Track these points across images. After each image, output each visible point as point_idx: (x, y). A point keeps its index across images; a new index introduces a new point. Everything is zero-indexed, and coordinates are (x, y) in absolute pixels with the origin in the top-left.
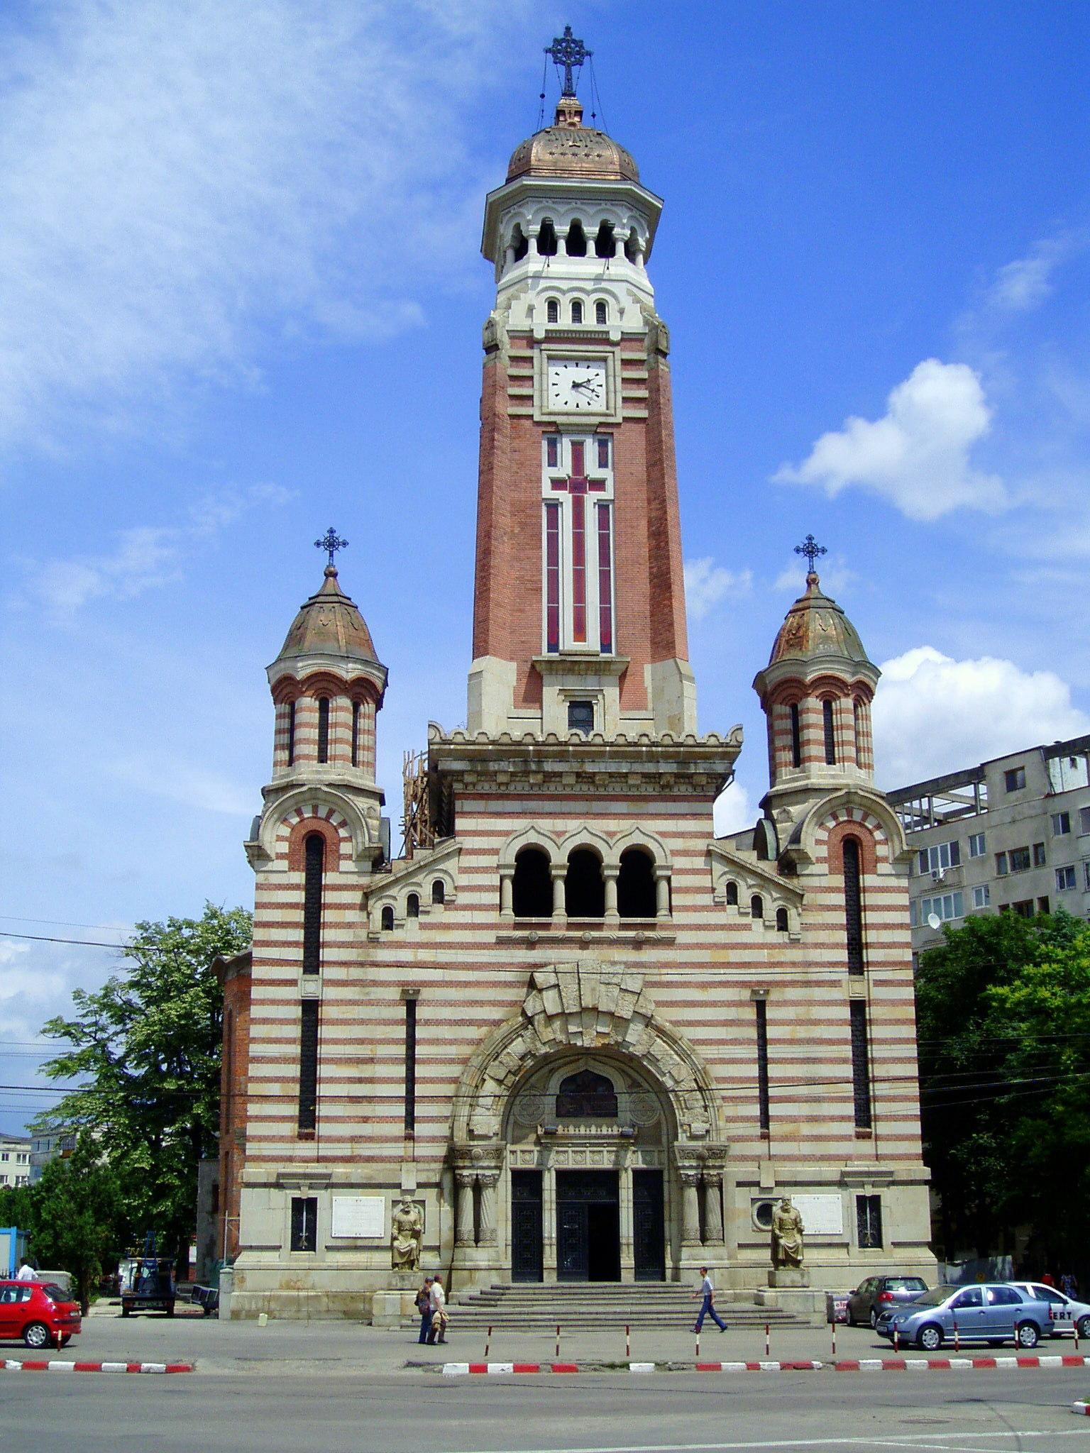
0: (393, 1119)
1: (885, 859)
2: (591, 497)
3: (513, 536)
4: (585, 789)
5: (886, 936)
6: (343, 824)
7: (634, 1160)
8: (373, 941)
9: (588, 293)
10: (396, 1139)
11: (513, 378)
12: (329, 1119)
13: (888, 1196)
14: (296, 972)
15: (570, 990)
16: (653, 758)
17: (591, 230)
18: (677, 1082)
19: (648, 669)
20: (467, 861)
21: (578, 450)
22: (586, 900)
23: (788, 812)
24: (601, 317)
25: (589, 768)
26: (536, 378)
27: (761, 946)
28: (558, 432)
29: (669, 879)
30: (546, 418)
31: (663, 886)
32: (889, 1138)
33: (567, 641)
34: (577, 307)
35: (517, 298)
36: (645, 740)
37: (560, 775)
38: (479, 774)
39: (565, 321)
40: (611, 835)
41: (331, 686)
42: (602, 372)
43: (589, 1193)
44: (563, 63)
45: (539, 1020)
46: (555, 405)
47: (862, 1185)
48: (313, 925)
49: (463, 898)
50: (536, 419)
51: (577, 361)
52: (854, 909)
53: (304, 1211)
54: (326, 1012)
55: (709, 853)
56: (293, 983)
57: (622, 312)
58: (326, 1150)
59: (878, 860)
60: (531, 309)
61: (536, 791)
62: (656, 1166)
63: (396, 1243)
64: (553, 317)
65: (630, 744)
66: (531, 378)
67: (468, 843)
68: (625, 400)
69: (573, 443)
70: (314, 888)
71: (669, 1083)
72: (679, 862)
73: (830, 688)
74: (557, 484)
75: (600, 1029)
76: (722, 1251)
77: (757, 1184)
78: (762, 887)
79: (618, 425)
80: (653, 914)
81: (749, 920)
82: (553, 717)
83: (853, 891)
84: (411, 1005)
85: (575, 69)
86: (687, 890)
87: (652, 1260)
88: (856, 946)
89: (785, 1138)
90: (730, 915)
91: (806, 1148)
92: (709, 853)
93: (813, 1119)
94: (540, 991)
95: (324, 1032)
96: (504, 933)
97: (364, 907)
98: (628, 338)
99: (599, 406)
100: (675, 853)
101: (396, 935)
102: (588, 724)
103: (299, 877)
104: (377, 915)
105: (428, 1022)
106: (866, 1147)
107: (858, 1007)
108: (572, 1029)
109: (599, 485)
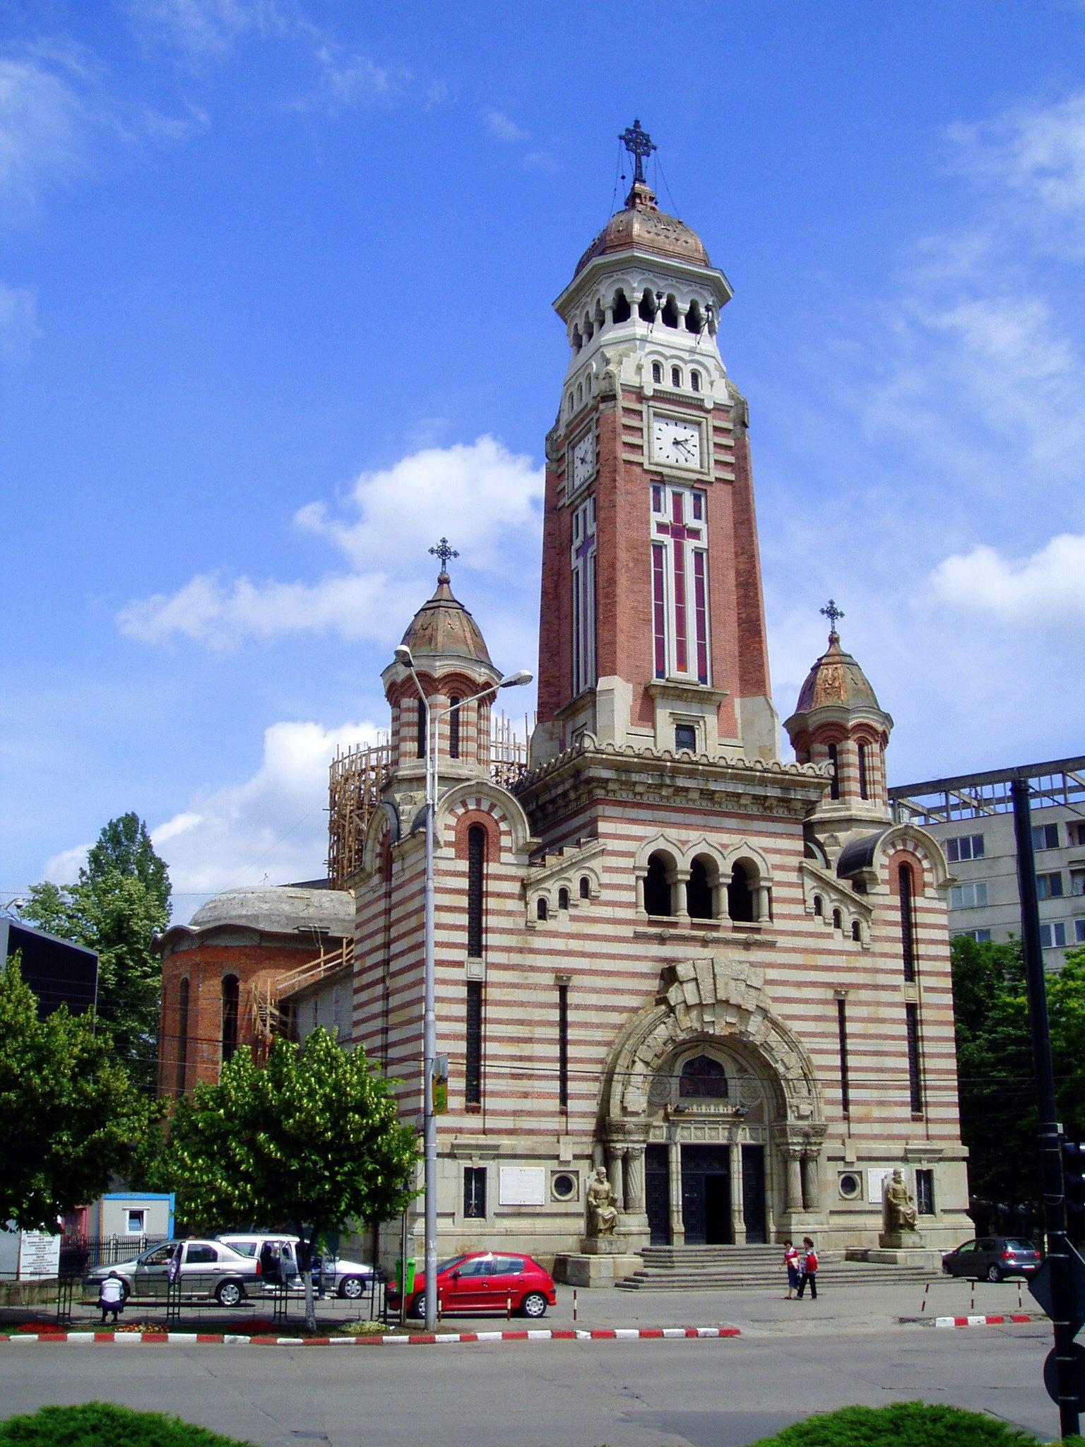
0: (548, 1096)
1: (930, 885)
2: (690, 545)
3: (628, 570)
4: (705, 805)
6: (504, 818)
7: (744, 1137)
8: (530, 930)
9: (686, 362)
11: (626, 427)
12: (495, 1094)
13: (939, 1170)
14: (462, 955)
15: (706, 986)
16: (763, 782)
17: (683, 306)
18: (787, 1068)
19: (737, 701)
21: (677, 498)
22: (701, 905)
23: (836, 838)
24: (695, 386)
25: (713, 786)
26: (645, 430)
27: (841, 953)
28: (663, 482)
29: (769, 889)
30: (653, 468)
31: (765, 894)
32: (936, 1121)
33: (672, 670)
34: (676, 372)
35: (627, 356)
36: (759, 766)
37: (687, 790)
38: (622, 783)
39: (667, 384)
40: (726, 845)
41: (463, 687)
42: (696, 434)
45: (680, 1009)
46: (659, 457)
47: (920, 1160)
48: (476, 911)
49: (606, 895)
50: (646, 466)
51: (677, 421)
52: (908, 925)
53: (476, 1178)
54: (491, 993)
55: (801, 869)
56: (459, 964)
57: (712, 383)
58: (491, 1123)
59: (925, 885)
60: (639, 368)
61: (665, 803)
62: (761, 1142)
63: (600, 1211)
64: (657, 379)
65: (747, 769)
66: (641, 430)
67: (613, 845)
68: (716, 461)
69: (675, 494)
70: (477, 876)
71: (781, 1069)
72: (779, 876)
74: (662, 528)
75: (729, 1020)
76: (822, 1217)
77: (843, 1159)
78: (840, 901)
79: (711, 483)
81: (831, 929)
82: (662, 738)
84: (563, 991)
85: (644, 158)
88: (909, 957)
89: (861, 1120)
90: (817, 924)
91: (877, 1129)
92: (801, 869)
93: (881, 1103)
94: (681, 983)
95: (489, 1012)
96: (640, 929)
97: (522, 897)
98: (719, 408)
99: (694, 463)
100: (776, 867)
101: (549, 925)
102: (692, 746)
103: (464, 865)
104: (534, 906)
105: (578, 1007)
106: (919, 1128)
107: (912, 1008)
108: (707, 1018)
109: (695, 534)
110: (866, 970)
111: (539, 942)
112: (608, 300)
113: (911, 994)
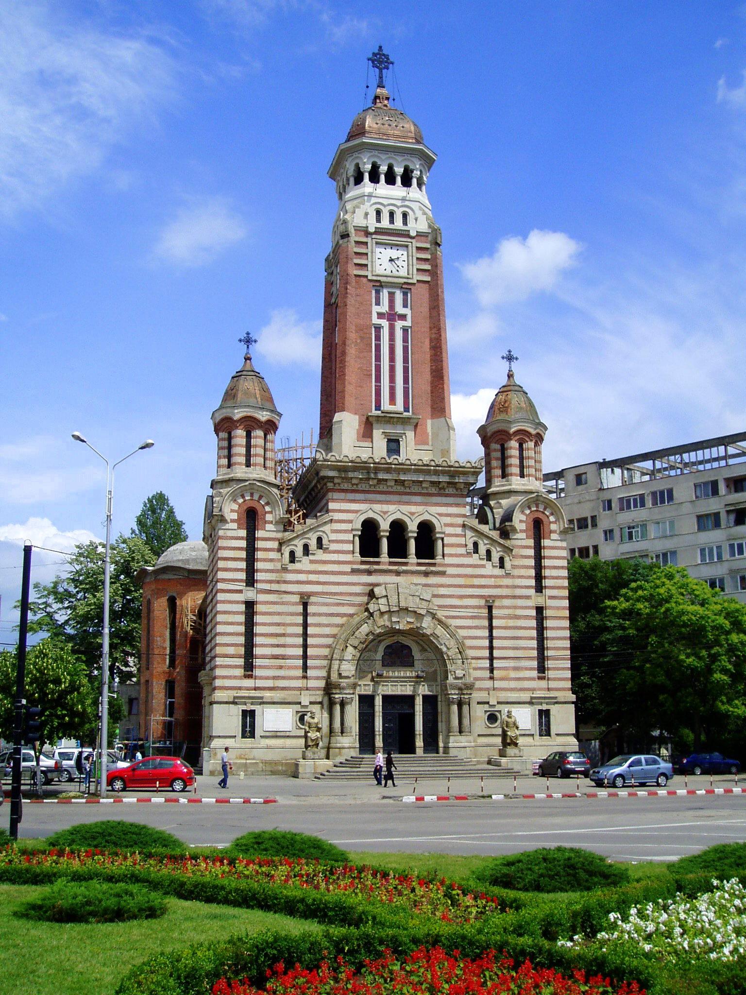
0: (296, 667)
1: (555, 532)
2: (399, 324)
3: (356, 344)
4: (399, 488)
5: (554, 573)
6: (268, 504)
7: (424, 690)
8: (284, 569)
9: (398, 207)
10: (297, 678)
11: (356, 253)
12: (261, 667)
13: (554, 710)
14: (242, 586)
15: (393, 600)
16: (436, 473)
17: (399, 170)
18: (448, 649)
19: (429, 422)
20: (336, 526)
21: (392, 296)
22: (398, 549)
23: (500, 503)
24: (405, 223)
25: (402, 477)
26: (369, 254)
27: (491, 577)
28: (381, 286)
29: (442, 539)
30: (375, 278)
31: (440, 542)
32: (555, 679)
33: (386, 406)
34: (392, 214)
35: (359, 207)
36: (433, 463)
37: (386, 480)
38: (343, 478)
39: (385, 223)
40: (412, 513)
41: (253, 424)
42: (405, 253)
43: (398, 706)
44: (377, 67)
45: (376, 614)
46: (379, 270)
47: (541, 704)
48: (251, 560)
49: (333, 547)
50: (369, 278)
51: (392, 246)
52: (539, 558)
53: (249, 716)
54: (259, 608)
55: (464, 526)
56: (240, 591)
57: (416, 219)
58: (260, 683)
59: (551, 532)
60: (366, 214)
61: (372, 489)
62: (435, 693)
63: (309, 734)
64: (378, 220)
65: (425, 465)
66: (367, 254)
67: (337, 516)
68: (418, 270)
69: (389, 293)
70: (251, 539)
71: (444, 649)
72: (449, 530)
73: (523, 436)
74: (380, 315)
75: (409, 620)
76: (471, 738)
77: (488, 703)
78: (492, 545)
79: (414, 284)
80: (432, 557)
81: (484, 562)
82: (379, 449)
83: (538, 548)
84: (305, 605)
85: (384, 71)
86: (452, 545)
87: (431, 744)
89: (502, 679)
90: (475, 559)
91: (513, 684)
92: (464, 526)
93: (516, 669)
94: (377, 599)
95: (258, 619)
96: (355, 567)
97: (279, 550)
98: (420, 235)
99: (403, 272)
100: (446, 525)
101: (297, 566)
102: (397, 452)
103: (243, 533)
104: (287, 555)
105: (314, 615)
106: (543, 684)
107: (540, 610)
108: (394, 619)
109: (403, 317)
110: (507, 587)
111: (290, 577)
113: (540, 600)
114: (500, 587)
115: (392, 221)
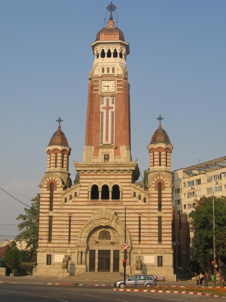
5: (166, 203)
10: (67, 243)
20: (82, 188)
21: (108, 100)
24: (113, 71)
27: (140, 205)
31: (121, 193)
33: (104, 142)
34: (108, 69)
39: (106, 72)
44: (110, 11)
46: (103, 91)
48: (51, 201)
49: (81, 196)
50: (99, 94)
52: (160, 198)
64: (103, 71)
67: (82, 184)
72: (125, 188)
80: (119, 198)
83: (160, 194)
86: (125, 194)
88: (160, 205)
89: (144, 244)
90: (134, 199)
91: (148, 246)
99: (112, 91)
104: (64, 199)
109: (112, 108)
110: (147, 209)
111: (65, 207)
112: (100, 52)
113: (160, 214)
114: (144, 209)
115: (108, 71)
